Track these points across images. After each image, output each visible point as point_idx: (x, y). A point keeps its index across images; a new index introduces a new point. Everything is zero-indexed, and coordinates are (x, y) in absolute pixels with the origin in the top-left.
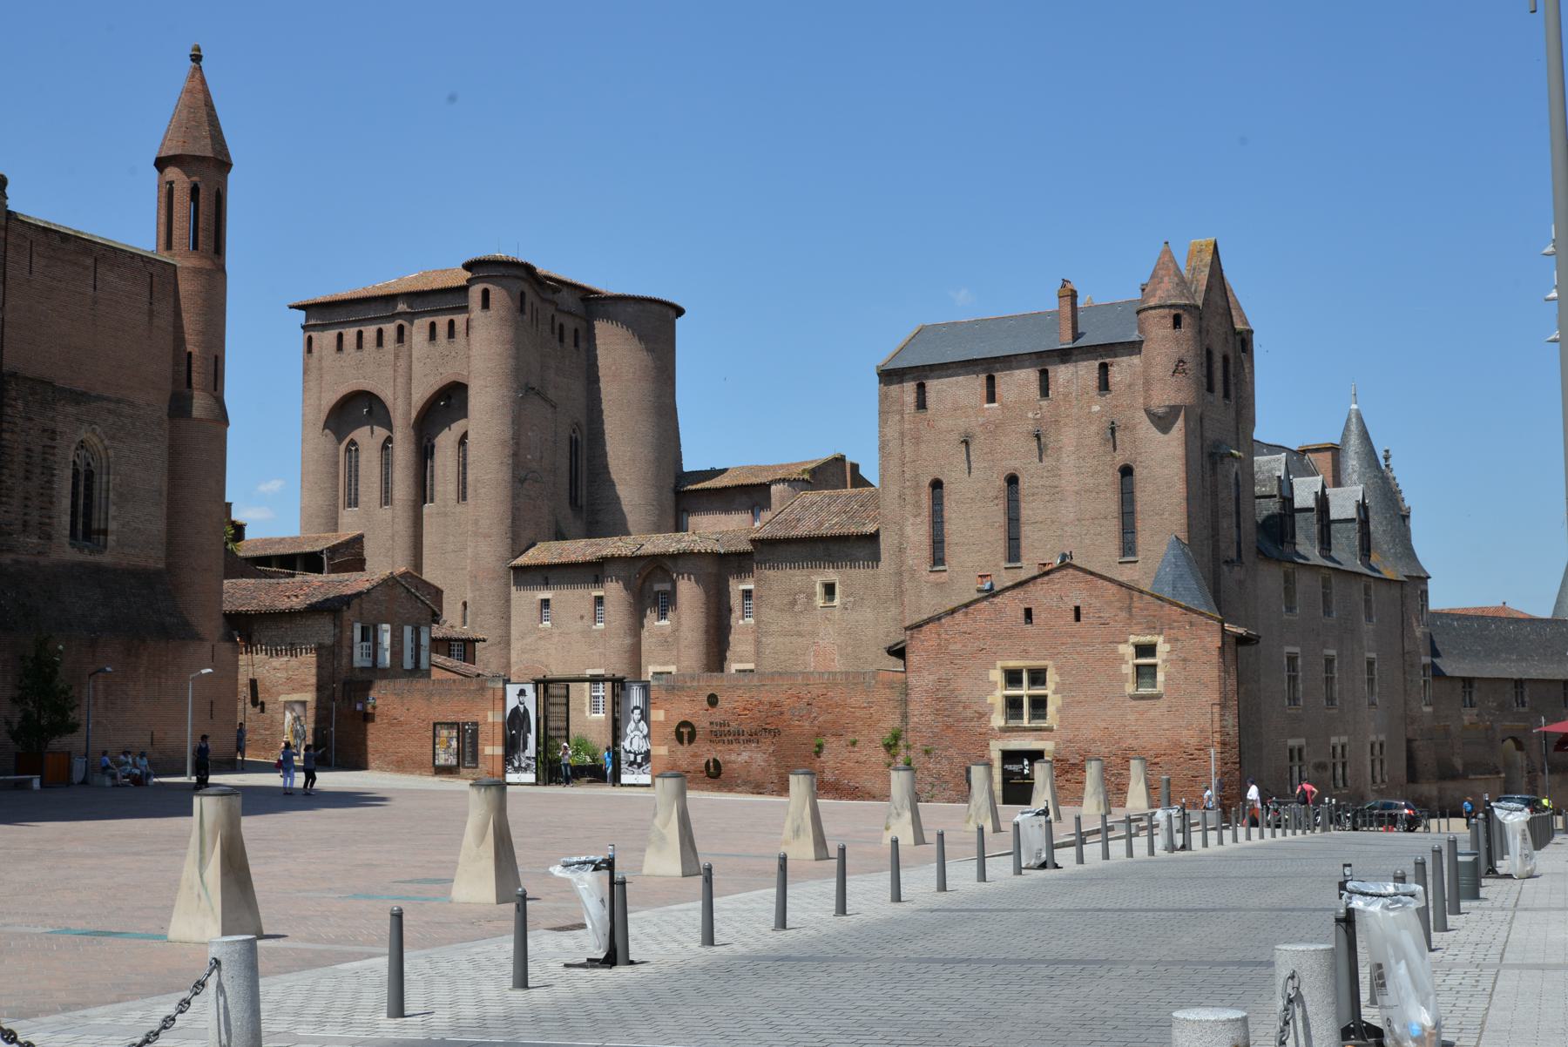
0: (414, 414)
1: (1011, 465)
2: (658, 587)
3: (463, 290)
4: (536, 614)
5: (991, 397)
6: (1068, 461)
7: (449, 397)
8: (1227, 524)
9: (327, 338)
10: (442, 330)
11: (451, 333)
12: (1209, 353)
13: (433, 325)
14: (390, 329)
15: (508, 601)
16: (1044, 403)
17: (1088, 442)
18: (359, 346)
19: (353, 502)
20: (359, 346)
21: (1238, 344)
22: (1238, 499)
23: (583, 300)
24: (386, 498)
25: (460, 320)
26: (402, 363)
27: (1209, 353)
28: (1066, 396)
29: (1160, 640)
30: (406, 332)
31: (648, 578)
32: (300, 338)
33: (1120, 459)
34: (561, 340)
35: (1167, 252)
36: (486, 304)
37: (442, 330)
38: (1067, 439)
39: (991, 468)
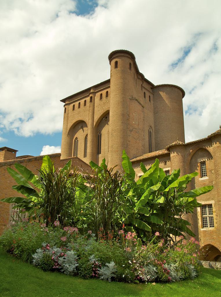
0: (94, 124)
11: (107, 96)
13: (101, 95)
14: (88, 99)
18: (79, 107)
20: (79, 107)
23: (152, 88)
26: (91, 108)
30: (93, 99)
31: (194, 156)
34: (145, 97)
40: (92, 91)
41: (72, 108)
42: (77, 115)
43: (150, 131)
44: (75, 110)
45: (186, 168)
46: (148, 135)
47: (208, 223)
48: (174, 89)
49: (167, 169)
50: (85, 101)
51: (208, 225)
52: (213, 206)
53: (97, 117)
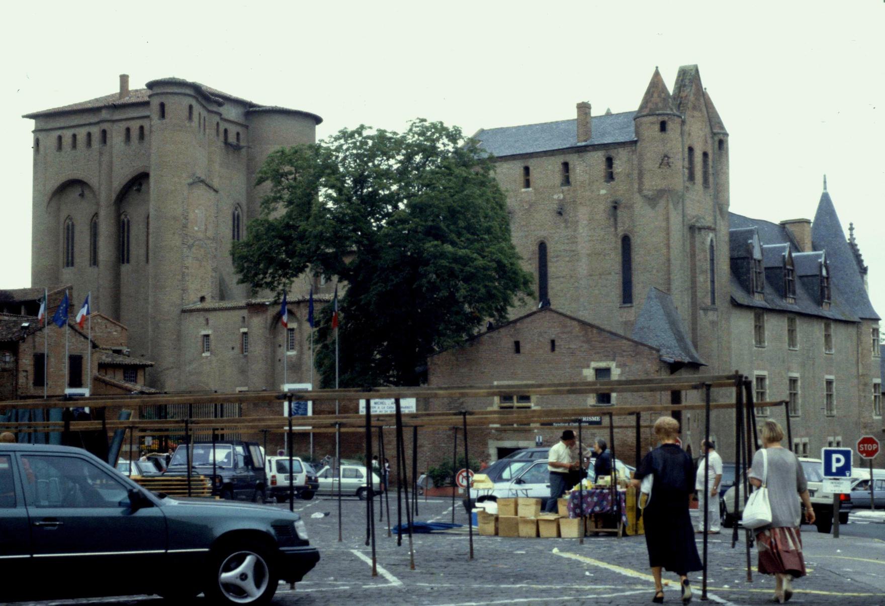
0: (114, 196)
1: (542, 234)
3: (146, 104)
5: (527, 184)
6: (583, 231)
7: (141, 185)
8: (703, 280)
10: (135, 133)
12: (691, 149)
13: (128, 130)
16: (565, 188)
17: (598, 217)
18: (74, 145)
19: (70, 263)
20: (74, 145)
21: (717, 143)
22: (712, 260)
24: (94, 261)
25: (146, 123)
27: (691, 149)
28: (582, 182)
29: (613, 365)
30: (108, 136)
33: (621, 231)
35: (657, 74)
36: (163, 115)
37: (135, 133)
38: (583, 214)
39: (526, 236)
40: (104, 115)
49: (245, 330)
53: (118, 183)
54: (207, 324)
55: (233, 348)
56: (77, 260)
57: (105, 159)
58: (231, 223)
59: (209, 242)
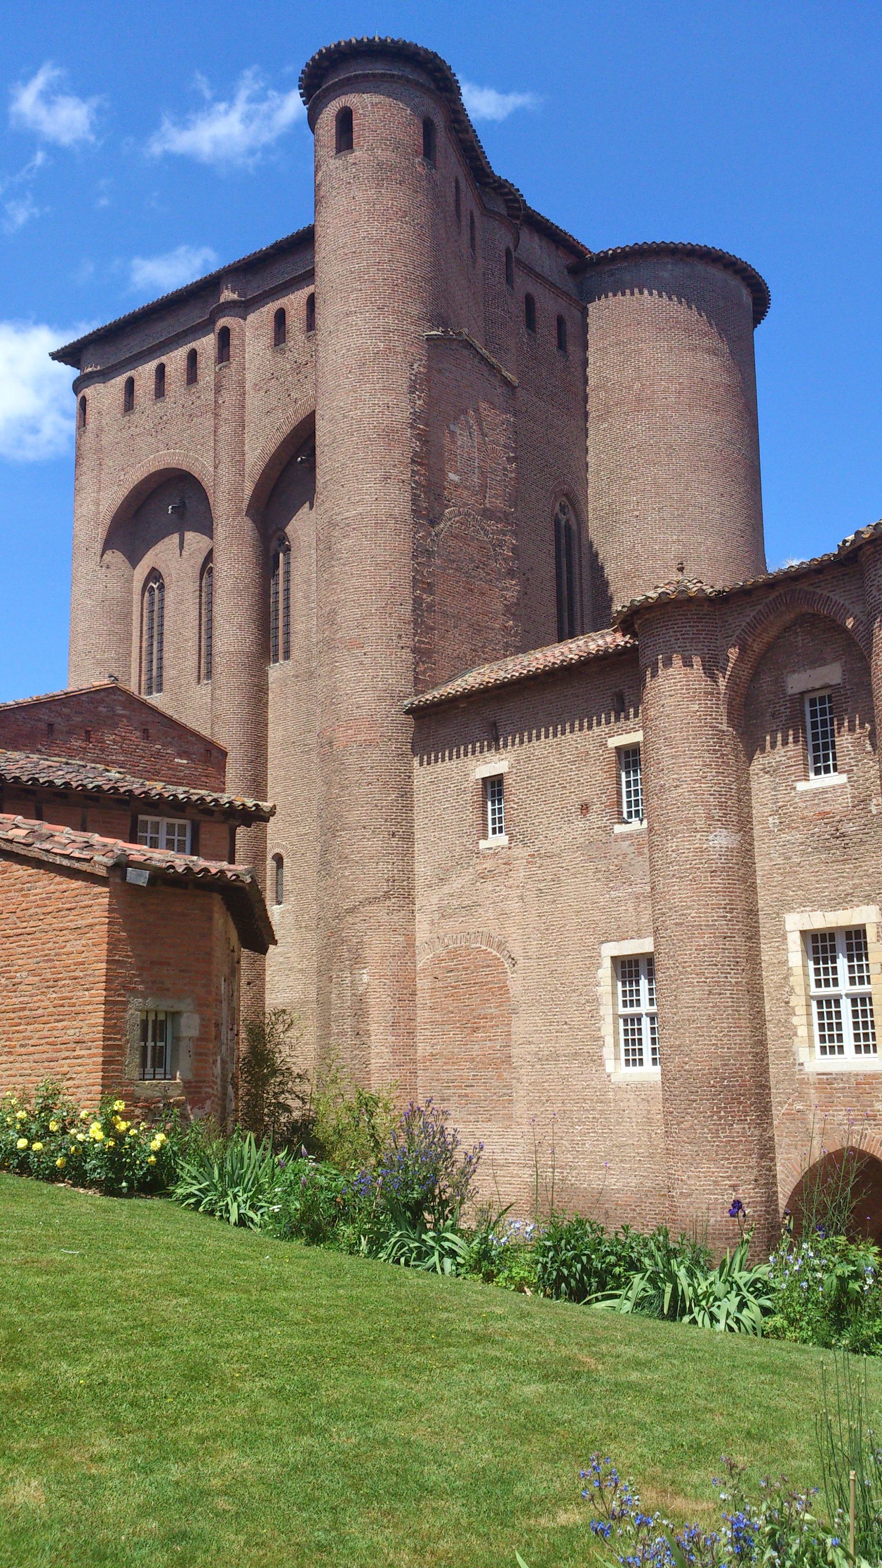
0: (249, 488)
2: (798, 682)
4: (471, 816)
9: (106, 395)
14: (207, 344)
15: (406, 794)
18: (160, 392)
20: (160, 392)
23: (573, 271)
30: (234, 341)
32: (72, 403)
34: (531, 322)
40: (228, 295)
41: (121, 397)
42: (150, 439)
43: (563, 523)
44: (138, 409)
45: (724, 727)
46: (552, 548)
47: (848, 1031)
48: (701, 268)
50: (193, 356)
51: (849, 1042)
52: (871, 936)
54: (497, 740)
55: (585, 808)
56: (169, 673)
57: (229, 398)
58: (550, 535)
59: (492, 526)
